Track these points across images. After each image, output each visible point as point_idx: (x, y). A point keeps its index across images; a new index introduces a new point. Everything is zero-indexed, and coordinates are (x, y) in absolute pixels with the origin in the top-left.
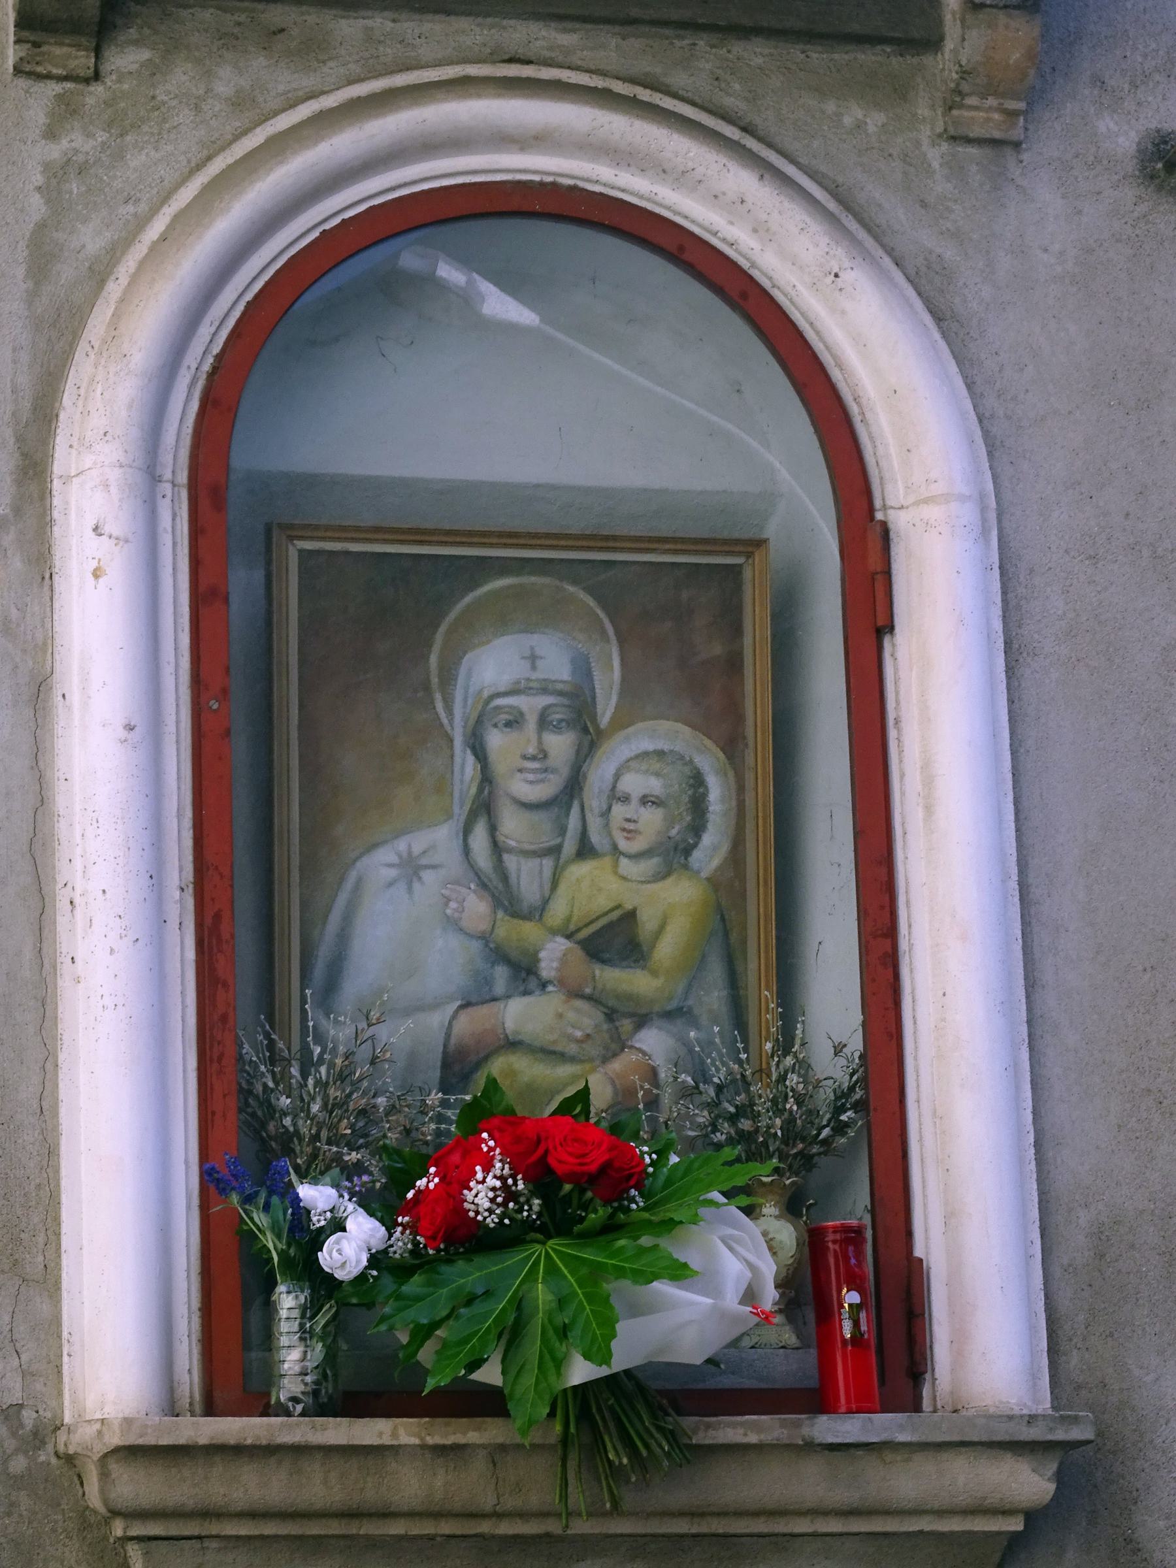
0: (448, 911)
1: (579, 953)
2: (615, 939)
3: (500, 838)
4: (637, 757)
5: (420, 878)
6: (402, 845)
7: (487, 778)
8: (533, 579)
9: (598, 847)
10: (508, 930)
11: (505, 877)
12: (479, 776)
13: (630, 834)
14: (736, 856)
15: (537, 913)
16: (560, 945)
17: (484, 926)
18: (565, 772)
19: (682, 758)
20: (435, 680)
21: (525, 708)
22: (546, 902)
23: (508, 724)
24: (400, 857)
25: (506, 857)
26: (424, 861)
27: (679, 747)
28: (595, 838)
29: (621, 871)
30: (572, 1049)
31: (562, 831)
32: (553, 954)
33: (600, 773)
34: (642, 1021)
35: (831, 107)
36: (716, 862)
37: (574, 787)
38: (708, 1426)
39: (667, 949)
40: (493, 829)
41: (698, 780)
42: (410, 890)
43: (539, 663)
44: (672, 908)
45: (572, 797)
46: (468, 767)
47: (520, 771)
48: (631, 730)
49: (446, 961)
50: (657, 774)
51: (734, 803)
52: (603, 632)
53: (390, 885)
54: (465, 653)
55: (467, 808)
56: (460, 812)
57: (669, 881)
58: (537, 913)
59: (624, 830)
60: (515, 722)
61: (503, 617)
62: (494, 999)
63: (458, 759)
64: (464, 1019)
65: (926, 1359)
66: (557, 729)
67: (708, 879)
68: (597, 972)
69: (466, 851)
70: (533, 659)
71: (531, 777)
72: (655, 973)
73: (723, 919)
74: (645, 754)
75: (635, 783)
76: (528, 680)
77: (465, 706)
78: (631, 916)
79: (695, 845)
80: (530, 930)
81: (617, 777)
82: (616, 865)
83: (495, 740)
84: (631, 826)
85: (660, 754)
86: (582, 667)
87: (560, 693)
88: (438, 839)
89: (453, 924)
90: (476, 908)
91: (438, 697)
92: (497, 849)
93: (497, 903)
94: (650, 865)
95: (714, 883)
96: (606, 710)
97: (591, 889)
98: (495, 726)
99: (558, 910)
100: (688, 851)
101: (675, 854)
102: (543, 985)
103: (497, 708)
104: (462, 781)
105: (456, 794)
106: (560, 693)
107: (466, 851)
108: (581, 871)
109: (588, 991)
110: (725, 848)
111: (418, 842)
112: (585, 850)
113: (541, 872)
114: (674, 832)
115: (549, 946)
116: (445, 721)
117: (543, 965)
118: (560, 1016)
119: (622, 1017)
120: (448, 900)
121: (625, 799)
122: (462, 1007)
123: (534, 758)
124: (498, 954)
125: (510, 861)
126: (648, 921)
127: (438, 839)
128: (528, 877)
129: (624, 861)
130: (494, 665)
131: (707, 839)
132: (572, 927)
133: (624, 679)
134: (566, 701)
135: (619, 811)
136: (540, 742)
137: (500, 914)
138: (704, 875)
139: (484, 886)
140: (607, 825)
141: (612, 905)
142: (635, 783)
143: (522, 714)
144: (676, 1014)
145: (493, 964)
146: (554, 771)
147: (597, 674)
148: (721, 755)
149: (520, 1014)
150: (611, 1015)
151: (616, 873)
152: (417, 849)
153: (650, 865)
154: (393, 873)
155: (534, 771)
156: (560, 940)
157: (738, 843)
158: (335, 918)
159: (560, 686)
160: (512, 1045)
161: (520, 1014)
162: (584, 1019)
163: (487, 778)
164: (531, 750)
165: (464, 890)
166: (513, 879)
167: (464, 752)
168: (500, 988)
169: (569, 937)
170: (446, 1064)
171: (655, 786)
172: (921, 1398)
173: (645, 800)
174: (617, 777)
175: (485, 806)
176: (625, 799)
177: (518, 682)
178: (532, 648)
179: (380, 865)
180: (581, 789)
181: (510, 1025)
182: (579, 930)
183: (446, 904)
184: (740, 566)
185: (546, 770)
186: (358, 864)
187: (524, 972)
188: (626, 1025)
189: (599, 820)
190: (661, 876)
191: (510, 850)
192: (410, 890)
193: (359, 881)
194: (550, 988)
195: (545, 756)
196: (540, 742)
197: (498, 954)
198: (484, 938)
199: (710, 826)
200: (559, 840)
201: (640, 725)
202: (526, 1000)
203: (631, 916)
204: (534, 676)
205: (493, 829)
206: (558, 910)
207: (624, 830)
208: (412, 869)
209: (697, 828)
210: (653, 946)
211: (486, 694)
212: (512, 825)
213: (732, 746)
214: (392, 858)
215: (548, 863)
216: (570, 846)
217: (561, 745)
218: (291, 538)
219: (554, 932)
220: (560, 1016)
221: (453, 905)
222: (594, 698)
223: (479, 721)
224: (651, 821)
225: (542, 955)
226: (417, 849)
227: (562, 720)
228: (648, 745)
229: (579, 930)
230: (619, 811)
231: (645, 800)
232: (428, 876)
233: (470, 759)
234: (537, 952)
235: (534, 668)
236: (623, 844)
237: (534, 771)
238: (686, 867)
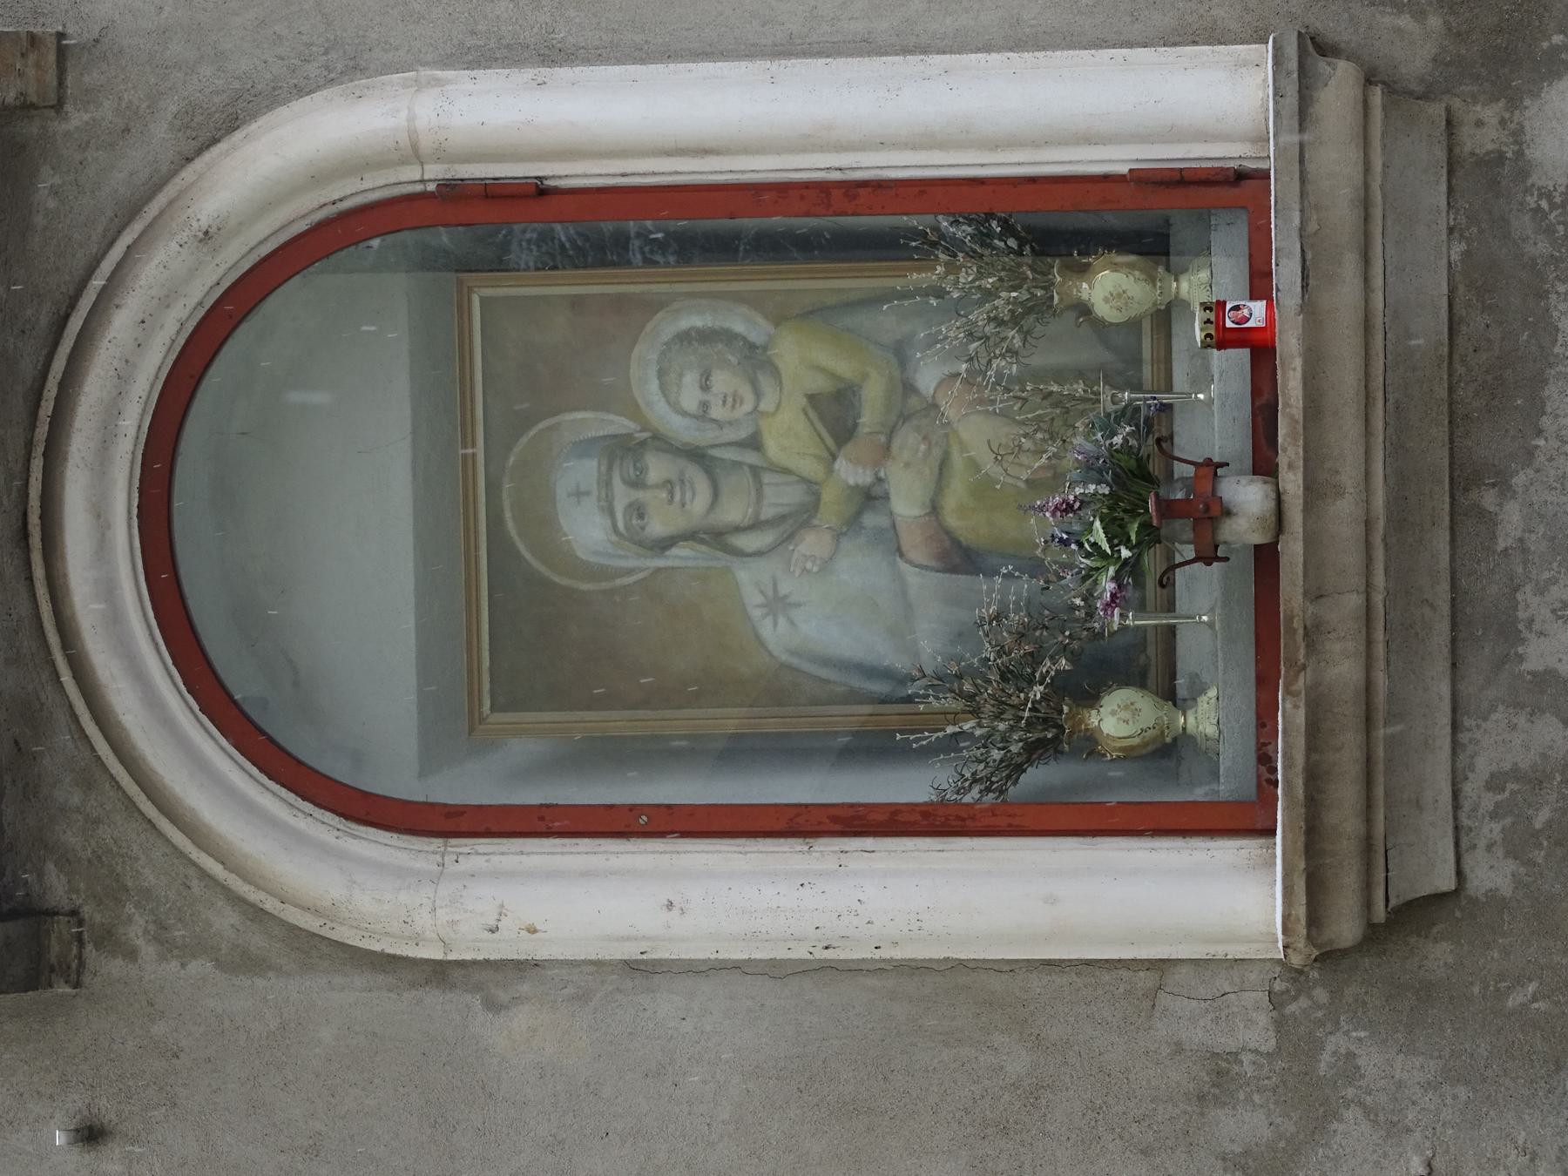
0: (815, 569)
1: (849, 447)
2: (835, 414)
3: (746, 522)
4: (665, 396)
5: (786, 596)
6: (756, 613)
7: (691, 536)
8: (505, 495)
9: (750, 431)
10: (831, 510)
11: (782, 518)
12: (691, 543)
13: (737, 400)
14: (755, 302)
15: (813, 488)
16: (841, 465)
17: (827, 538)
18: (682, 463)
19: (663, 353)
20: (604, 585)
21: (626, 501)
22: (804, 480)
23: (641, 516)
24: (765, 616)
25: (763, 517)
26: (770, 593)
27: (654, 357)
28: (743, 434)
29: (771, 408)
30: (937, 452)
31: (737, 465)
32: (851, 472)
33: (680, 428)
34: (909, 388)
35: (39, 220)
36: (760, 320)
37: (697, 455)
38: (1287, 405)
39: (845, 368)
40: (738, 529)
41: (685, 337)
42: (797, 605)
43: (583, 489)
44: (805, 359)
45: (704, 456)
46: (682, 554)
47: (683, 505)
48: (640, 401)
49: (859, 569)
50: (681, 375)
51: (704, 302)
52: (550, 428)
53: (792, 623)
54: (577, 558)
55: (720, 554)
56: (723, 560)
57: (781, 366)
58: (813, 488)
59: (733, 407)
60: (638, 510)
61: (543, 524)
62: (894, 526)
63: (677, 563)
64: (913, 555)
65: (1222, 169)
66: (643, 471)
67: (777, 325)
68: (866, 430)
69: (759, 554)
70: (579, 494)
71: (688, 495)
72: (865, 376)
73: (811, 312)
74: (663, 387)
75: (690, 398)
76: (599, 500)
77: (627, 557)
78: (812, 398)
79: (744, 338)
80: (829, 495)
81: (685, 414)
82: (764, 414)
83: (657, 527)
84: (730, 400)
85: (661, 374)
86: (584, 448)
87: (610, 468)
88: (750, 580)
89: (827, 565)
90: (812, 544)
91: (619, 582)
92: (756, 525)
93: (806, 524)
94: (765, 381)
95: (779, 320)
96: (620, 424)
97: (790, 436)
98: (643, 528)
99: (809, 467)
100: (752, 347)
101: (756, 360)
102: (880, 480)
103: (627, 528)
104: (695, 558)
105: (706, 564)
106: (610, 468)
107: (759, 554)
108: (773, 448)
109: (883, 439)
110: (744, 309)
111: (753, 598)
112: (754, 443)
113: (777, 485)
114: (734, 360)
115: (843, 475)
116: (640, 576)
117: (860, 481)
118: (907, 465)
119: (907, 405)
120: (804, 569)
121: (705, 405)
122: (902, 555)
123: (671, 494)
124: (853, 523)
125: (767, 513)
126: (820, 384)
127: (750, 580)
128: (781, 497)
129: (763, 407)
130: (587, 530)
131: (739, 327)
132: (825, 454)
133: (595, 408)
134: (617, 463)
135: (717, 412)
136: (656, 486)
137: (816, 522)
138: (772, 330)
139: (790, 537)
140: (730, 423)
141: (802, 417)
142: (690, 398)
143: (630, 505)
144: (900, 353)
145: (861, 528)
146: (682, 473)
147: (592, 433)
148: (660, 315)
149: (906, 504)
150: (905, 417)
151: (774, 414)
152: (760, 599)
153: (765, 381)
154: (782, 621)
155: (683, 494)
156: (837, 465)
157: (738, 298)
158: (825, 673)
159: (603, 468)
160: (935, 509)
161: (906, 504)
162: (908, 441)
163: (691, 536)
164: (664, 495)
165: (796, 555)
166: (780, 510)
167: (667, 557)
168: (883, 521)
169: (834, 457)
170: (953, 570)
171: (691, 379)
172: (1256, 170)
173: (705, 387)
174: (685, 414)
175: (716, 537)
176: (705, 405)
177: (602, 509)
178: (569, 495)
179: (776, 636)
180: (698, 447)
181: (916, 512)
182: (828, 449)
183: (809, 571)
184: (483, 300)
185: (682, 481)
186: (776, 653)
187: (871, 497)
188: (914, 401)
189: (725, 431)
190: (776, 373)
191: (757, 513)
192: (797, 605)
193: (792, 653)
194: (882, 474)
195: (669, 482)
196: (656, 486)
197: (853, 523)
198: (838, 536)
199: (727, 325)
200: (746, 469)
201: (636, 393)
202: (893, 498)
203: (812, 398)
204: (595, 493)
205: (738, 529)
206: (809, 467)
207: (733, 407)
208: (777, 604)
209: (728, 337)
210: (839, 378)
211: (614, 538)
212: (734, 511)
213: (652, 306)
214: (768, 621)
215: (767, 478)
216: (750, 457)
217: (657, 468)
218: (482, 720)
219: (830, 471)
220: (907, 465)
221: (809, 565)
222: (615, 436)
223: (640, 544)
224: (723, 381)
225: (851, 482)
226: (760, 599)
227: (636, 469)
228: (654, 385)
229: (828, 449)
230: (717, 412)
231: (705, 387)
232: (785, 588)
233: (675, 551)
234: (850, 487)
235: (588, 493)
236: (748, 406)
237: (683, 494)
238: (765, 348)
